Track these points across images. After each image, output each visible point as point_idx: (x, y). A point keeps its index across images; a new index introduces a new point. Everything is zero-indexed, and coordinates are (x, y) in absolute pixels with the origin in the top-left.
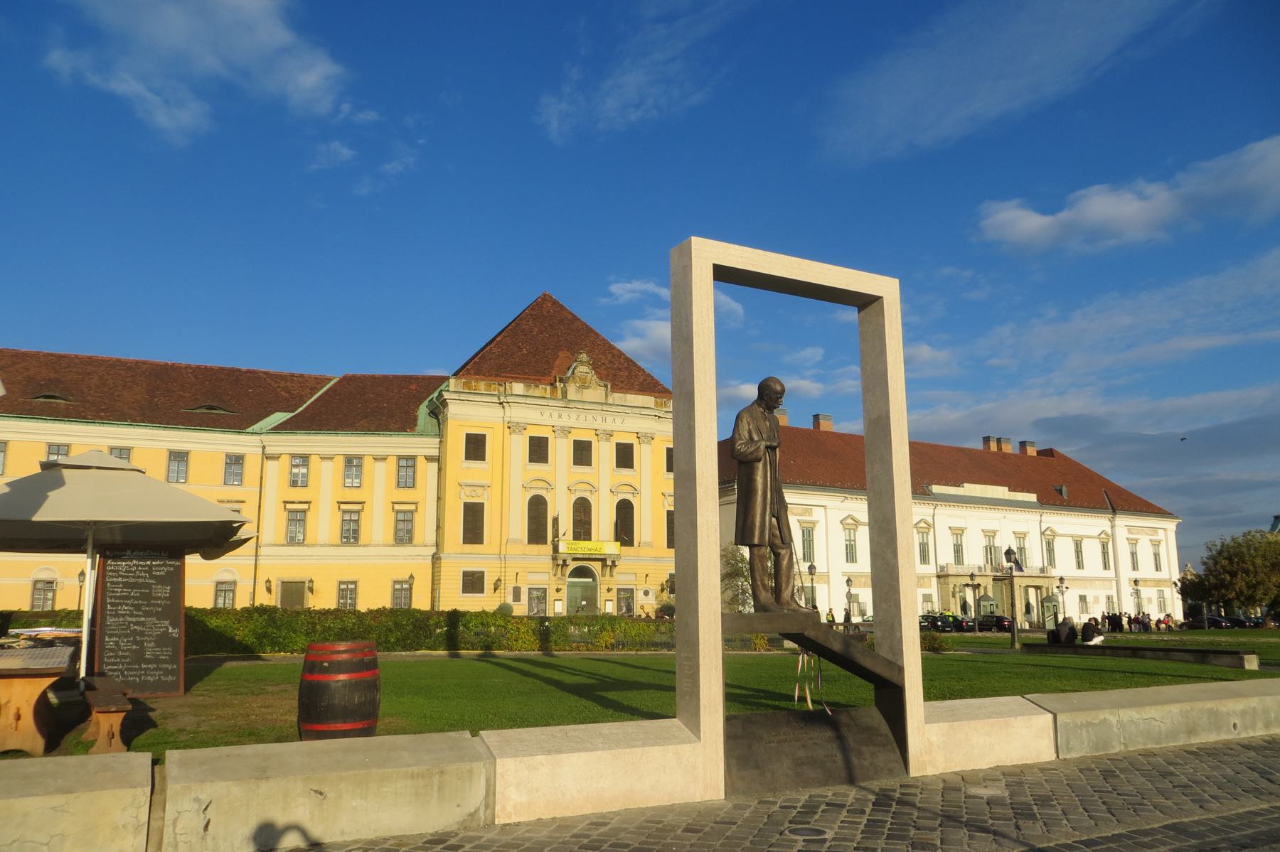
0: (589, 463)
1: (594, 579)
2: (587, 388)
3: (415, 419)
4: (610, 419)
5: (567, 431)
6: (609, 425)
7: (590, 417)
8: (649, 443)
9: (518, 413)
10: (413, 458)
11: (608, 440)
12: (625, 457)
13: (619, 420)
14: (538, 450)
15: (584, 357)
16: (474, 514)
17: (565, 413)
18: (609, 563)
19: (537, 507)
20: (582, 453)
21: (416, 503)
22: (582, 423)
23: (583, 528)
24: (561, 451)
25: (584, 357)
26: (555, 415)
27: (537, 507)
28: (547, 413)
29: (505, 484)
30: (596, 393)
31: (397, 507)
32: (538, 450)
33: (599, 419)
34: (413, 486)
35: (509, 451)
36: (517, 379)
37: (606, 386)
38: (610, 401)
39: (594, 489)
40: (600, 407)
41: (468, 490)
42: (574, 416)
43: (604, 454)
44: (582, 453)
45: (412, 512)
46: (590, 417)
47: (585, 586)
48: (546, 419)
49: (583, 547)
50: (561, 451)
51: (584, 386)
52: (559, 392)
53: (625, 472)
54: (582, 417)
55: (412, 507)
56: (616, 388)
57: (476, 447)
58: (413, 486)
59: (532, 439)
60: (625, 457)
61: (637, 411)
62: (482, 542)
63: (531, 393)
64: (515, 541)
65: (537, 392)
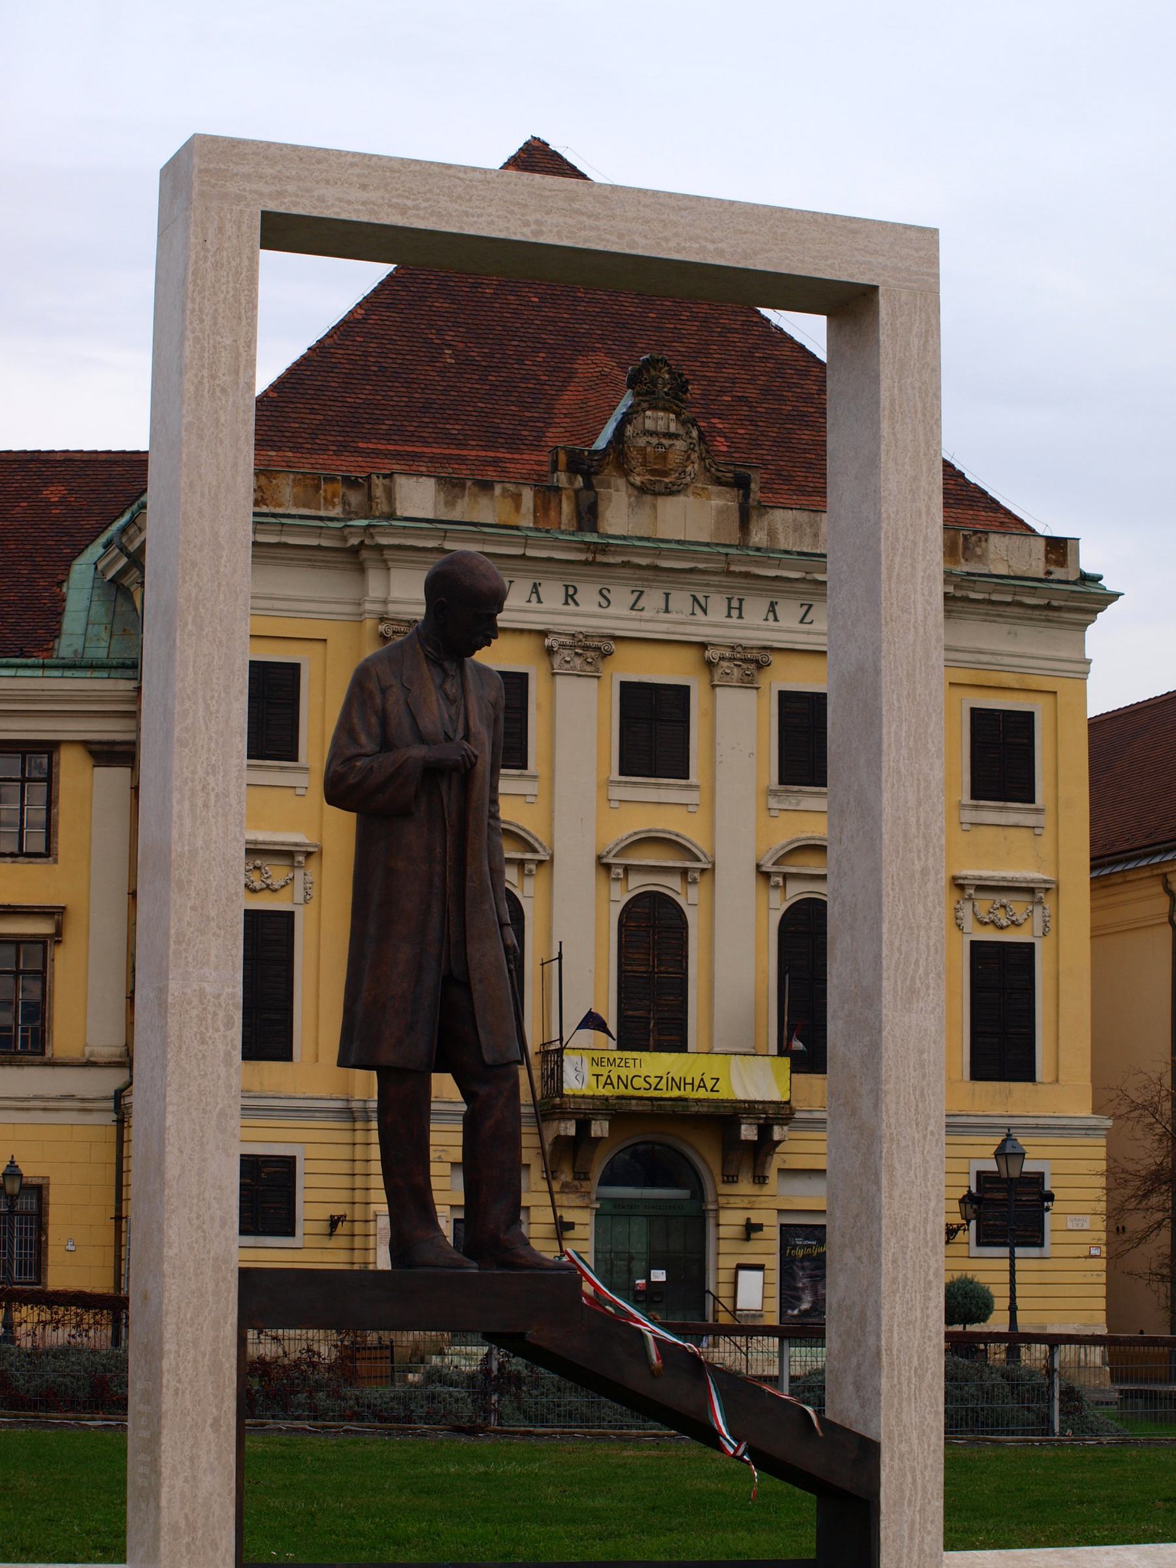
0: (678, 768)
1: (699, 1194)
2: (670, 492)
3: (53, 613)
4: (755, 608)
6: (754, 626)
7: (681, 600)
10: (50, 748)
11: (748, 682)
18: (748, 1132)
21: (55, 913)
23: (653, 1001)
34: (48, 853)
36: (413, 465)
39: (695, 867)
45: (41, 941)
47: (659, 1213)
49: (653, 1071)
54: (653, 599)
55: (43, 927)
58: (48, 853)
63: (463, 509)
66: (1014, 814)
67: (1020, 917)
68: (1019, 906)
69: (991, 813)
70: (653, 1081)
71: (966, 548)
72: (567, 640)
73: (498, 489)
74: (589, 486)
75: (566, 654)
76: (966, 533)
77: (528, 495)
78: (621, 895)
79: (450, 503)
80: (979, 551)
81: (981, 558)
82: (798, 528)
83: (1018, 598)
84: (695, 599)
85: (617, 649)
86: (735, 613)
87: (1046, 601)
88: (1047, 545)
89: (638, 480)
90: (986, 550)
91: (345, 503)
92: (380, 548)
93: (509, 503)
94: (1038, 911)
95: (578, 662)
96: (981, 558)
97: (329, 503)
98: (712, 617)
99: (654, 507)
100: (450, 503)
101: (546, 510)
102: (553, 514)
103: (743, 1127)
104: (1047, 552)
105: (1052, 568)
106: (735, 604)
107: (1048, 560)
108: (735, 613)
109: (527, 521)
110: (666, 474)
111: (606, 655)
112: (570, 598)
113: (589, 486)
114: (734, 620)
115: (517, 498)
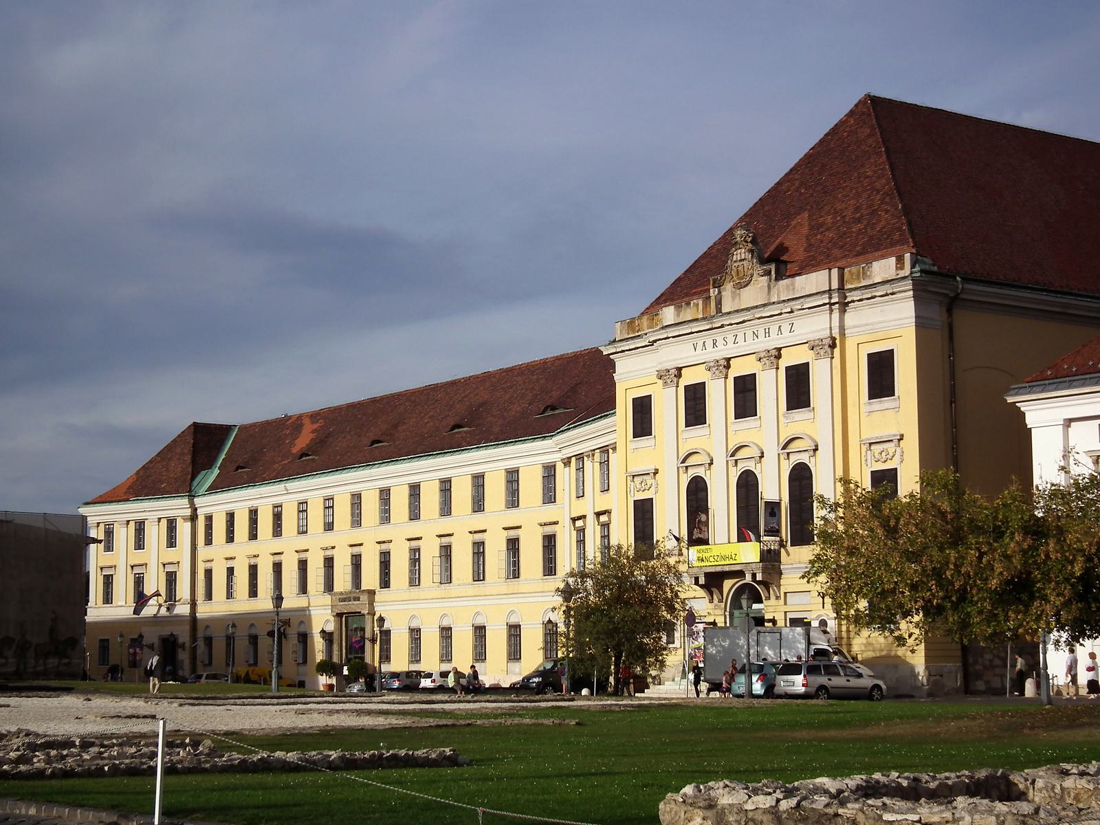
17: (719, 336)
22: (743, 346)
37: (768, 273)
60: (798, 389)
65: (688, 314)
66: (886, 402)
70: (716, 558)
71: (864, 273)
74: (720, 292)
76: (863, 265)
79: (678, 315)
80: (868, 273)
81: (869, 277)
83: (874, 294)
84: (754, 332)
86: (767, 335)
87: (885, 292)
88: (897, 260)
90: (871, 272)
96: (869, 277)
99: (739, 294)
100: (678, 315)
102: (708, 309)
103: (747, 575)
104: (897, 264)
105: (899, 272)
106: (767, 331)
107: (897, 269)
108: (767, 335)
113: (720, 292)
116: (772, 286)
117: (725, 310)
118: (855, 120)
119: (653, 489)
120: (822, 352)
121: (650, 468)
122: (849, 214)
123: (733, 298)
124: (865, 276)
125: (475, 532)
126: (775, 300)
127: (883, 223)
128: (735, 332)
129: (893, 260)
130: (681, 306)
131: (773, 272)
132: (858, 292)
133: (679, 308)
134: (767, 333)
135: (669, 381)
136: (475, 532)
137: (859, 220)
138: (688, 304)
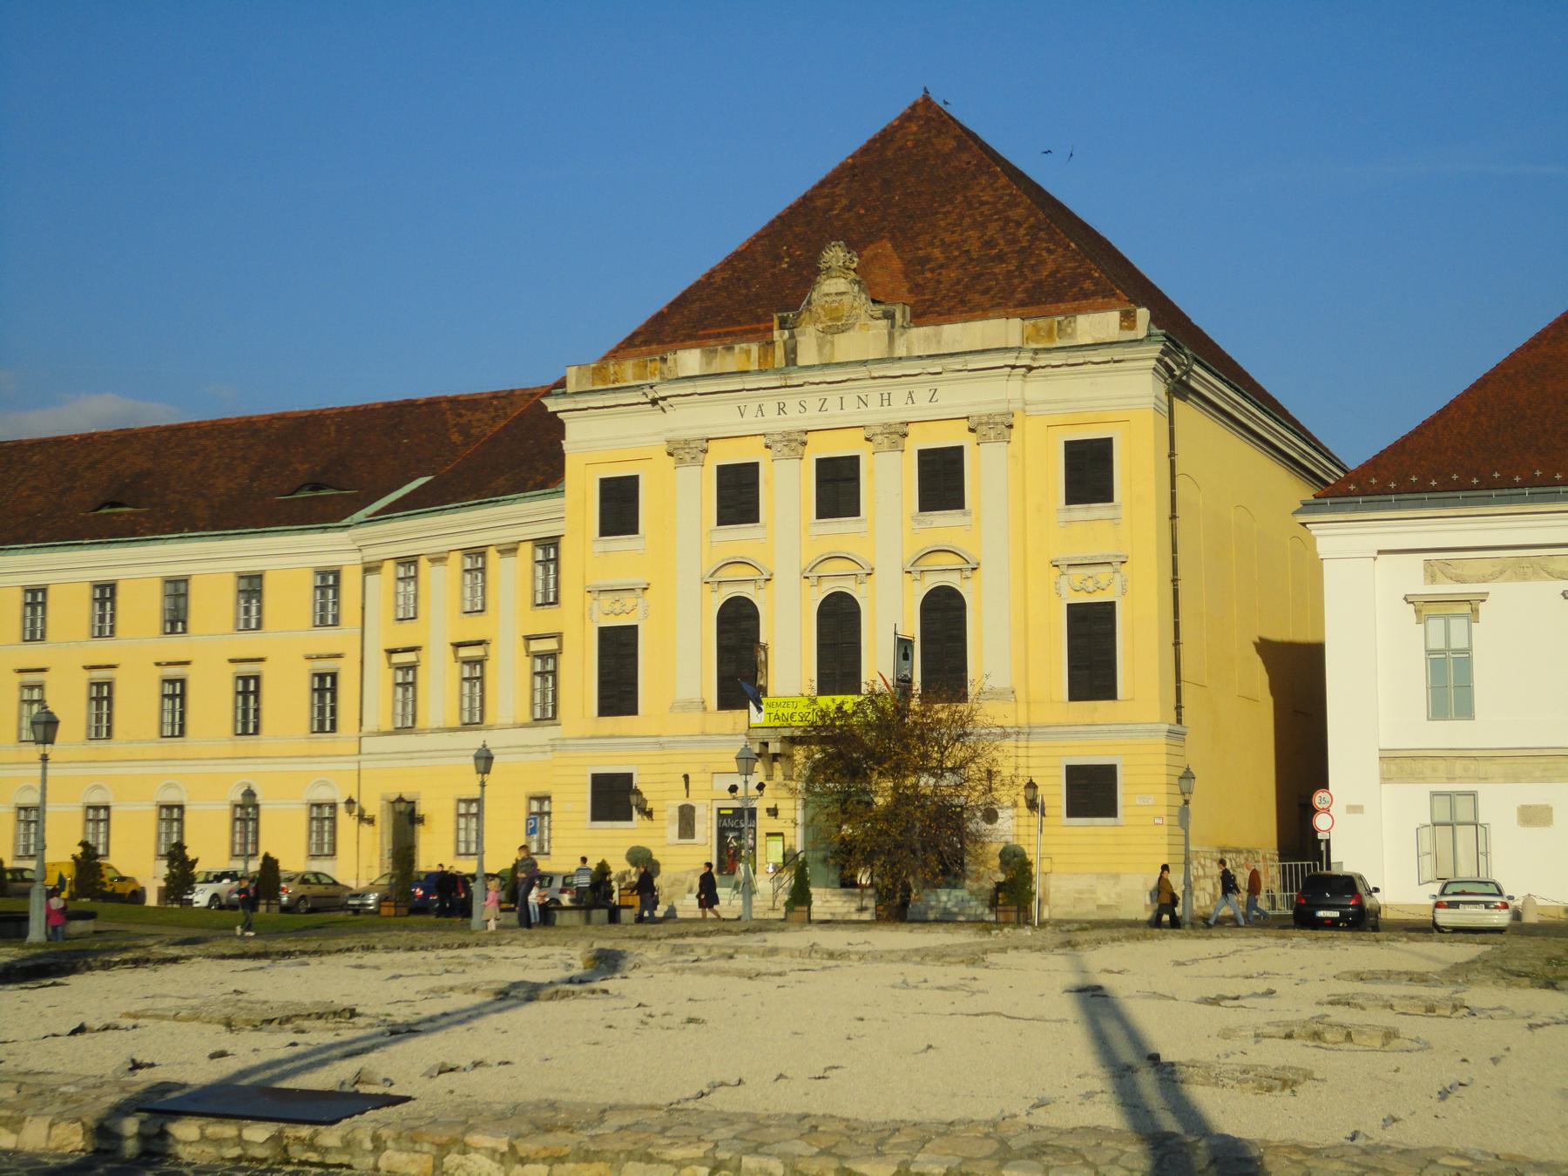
4: (899, 395)
5: (795, 442)
8: (1000, 437)
9: (691, 417)
11: (896, 447)
12: (941, 480)
13: (922, 394)
14: (738, 495)
15: (835, 255)
16: (618, 653)
17: (791, 400)
19: (738, 629)
20: (838, 488)
21: (558, 636)
24: (788, 489)
25: (835, 255)
26: (770, 407)
27: (738, 629)
28: (753, 407)
29: (671, 580)
30: (865, 338)
31: (536, 646)
32: (738, 495)
33: (874, 399)
35: (679, 501)
37: (889, 316)
38: (900, 351)
40: (861, 372)
41: (607, 600)
42: (813, 403)
43: (889, 482)
44: (838, 488)
46: (851, 400)
48: (751, 423)
50: (788, 489)
51: (837, 325)
52: (779, 353)
53: (943, 520)
56: (920, 316)
57: (619, 506)
59: (722, 470)
60: (941, 480)
61: (956, 363)
62: (633, 711)
64: (686, 706)
66: (1098, 510)
67: (1103, 584)
68: (1103, 574)
69: (1080, 511)
71: (1060, 330)
72: (777, 438)
73: (737, 348)
74: (792, 336)
75: (779, 446)
77: (754, 348)
78: (819, 595)
79: (709, 364)
81: (1071, 336)
82: (927, 338)
85: (809, 437)
89: (820, 327)
90: (1074, 330)
91: (662, 373)
92: (664, 399)
93: (744, 356)
94: (1117, 576)
95: (786, 450)
97: (653, 374)
98: (870, 408)
99: (832, 343)
100: (709, 364)
101: (766, 356)
107: (1122, 327)
109: (754, 367)
110: (839, 319)
111: (804, 443)
112: (781, 410)
113: (792, 336)
114: (886, 407)
115: (748, 352)
116: (897, 334)
117: (801, 362)
118: (921, 127)
119: (640, 610)
120: (992, 434)
121: (637, 580)
122: (974, 247)
123: (820, 347)
124: (1061, 331)
125: (169, 664)
126: (904, 354)
127: (1051, 266)
128: (841, 394)
129: (1114, 316)
130: (715, 351)
131: (898, 316)
132: (1063, 354)
133: (710, 354)
134: (886, 400)
135: (687, 457)
136: (169, 664)
137: (1001, 258)
138: (730, 349)
